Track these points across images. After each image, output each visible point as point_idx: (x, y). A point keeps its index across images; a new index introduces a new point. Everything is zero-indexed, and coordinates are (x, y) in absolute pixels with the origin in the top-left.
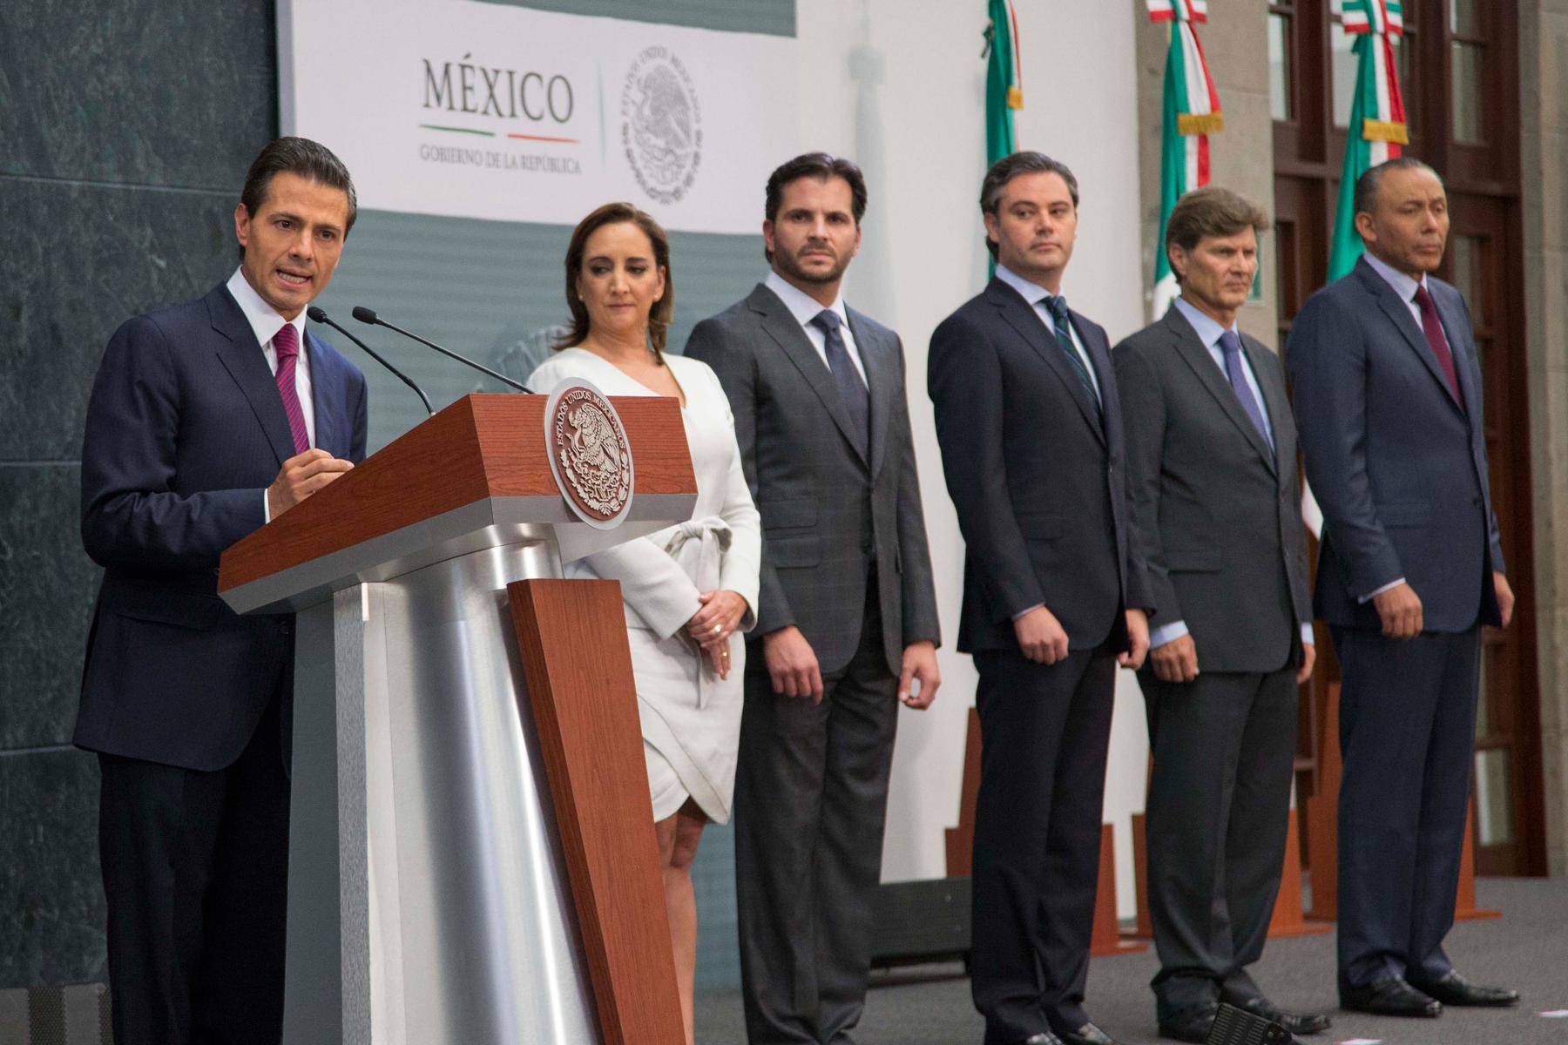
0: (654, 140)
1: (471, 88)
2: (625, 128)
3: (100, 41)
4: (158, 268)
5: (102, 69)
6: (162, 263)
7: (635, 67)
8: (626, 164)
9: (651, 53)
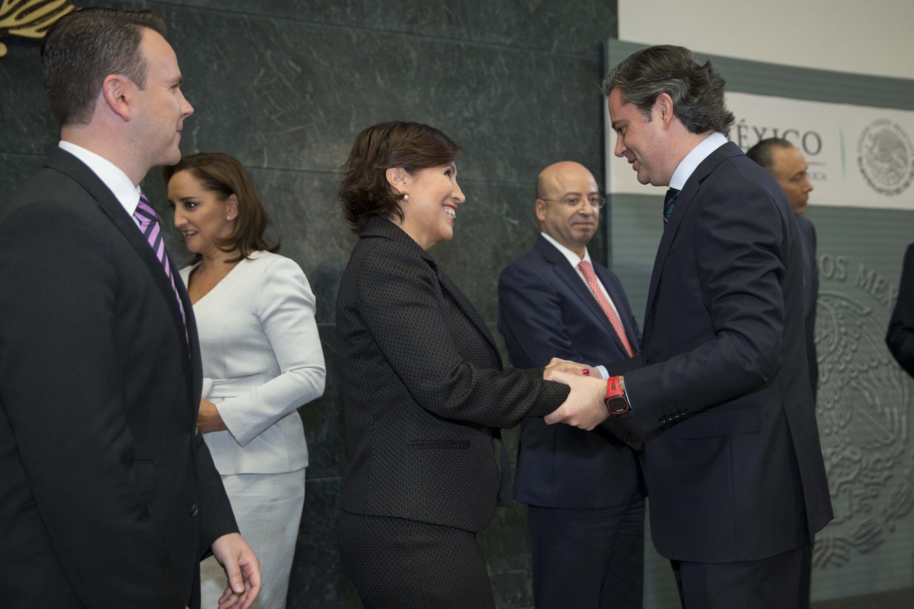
0: (880, 164)
1: (745, 137)
2: (860, 159)
3: (471, 110)
4: (514, 226)
5: (472, 124)
6: (516, 222)
7: (867, 129)
8: (860, 176)
9: (878, 123)
